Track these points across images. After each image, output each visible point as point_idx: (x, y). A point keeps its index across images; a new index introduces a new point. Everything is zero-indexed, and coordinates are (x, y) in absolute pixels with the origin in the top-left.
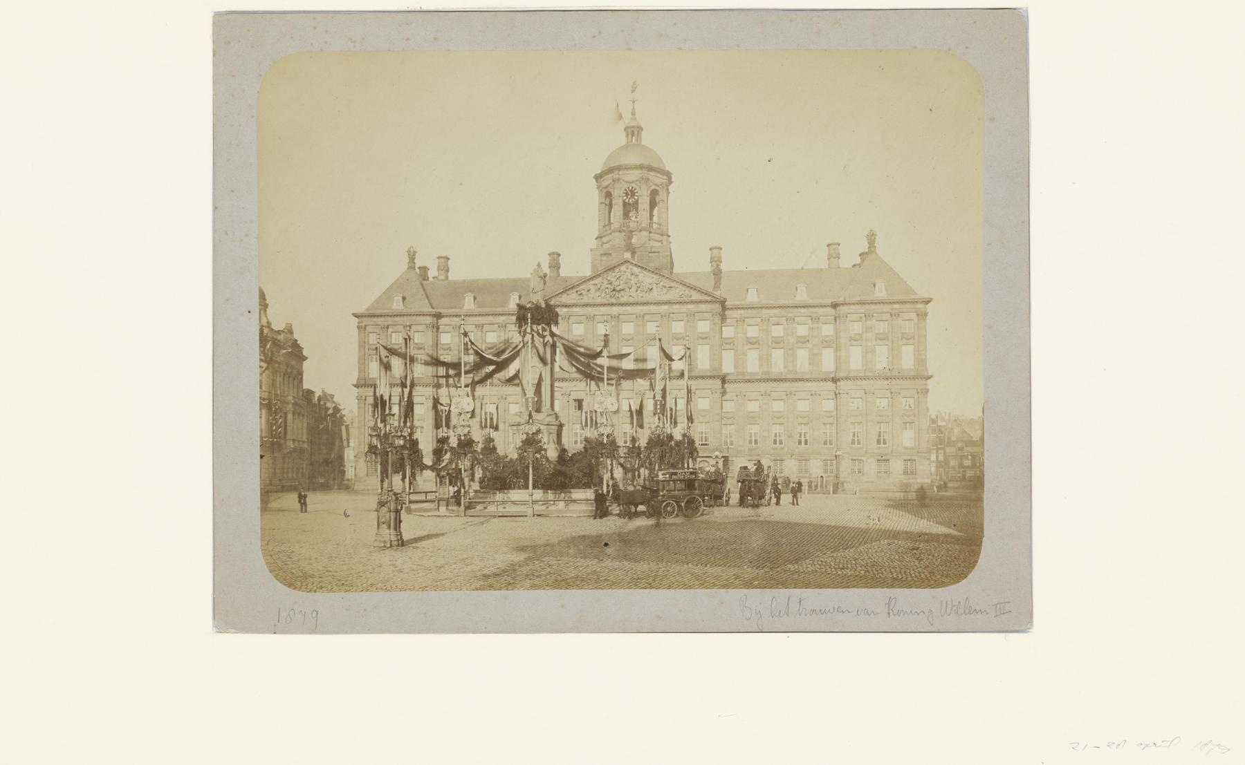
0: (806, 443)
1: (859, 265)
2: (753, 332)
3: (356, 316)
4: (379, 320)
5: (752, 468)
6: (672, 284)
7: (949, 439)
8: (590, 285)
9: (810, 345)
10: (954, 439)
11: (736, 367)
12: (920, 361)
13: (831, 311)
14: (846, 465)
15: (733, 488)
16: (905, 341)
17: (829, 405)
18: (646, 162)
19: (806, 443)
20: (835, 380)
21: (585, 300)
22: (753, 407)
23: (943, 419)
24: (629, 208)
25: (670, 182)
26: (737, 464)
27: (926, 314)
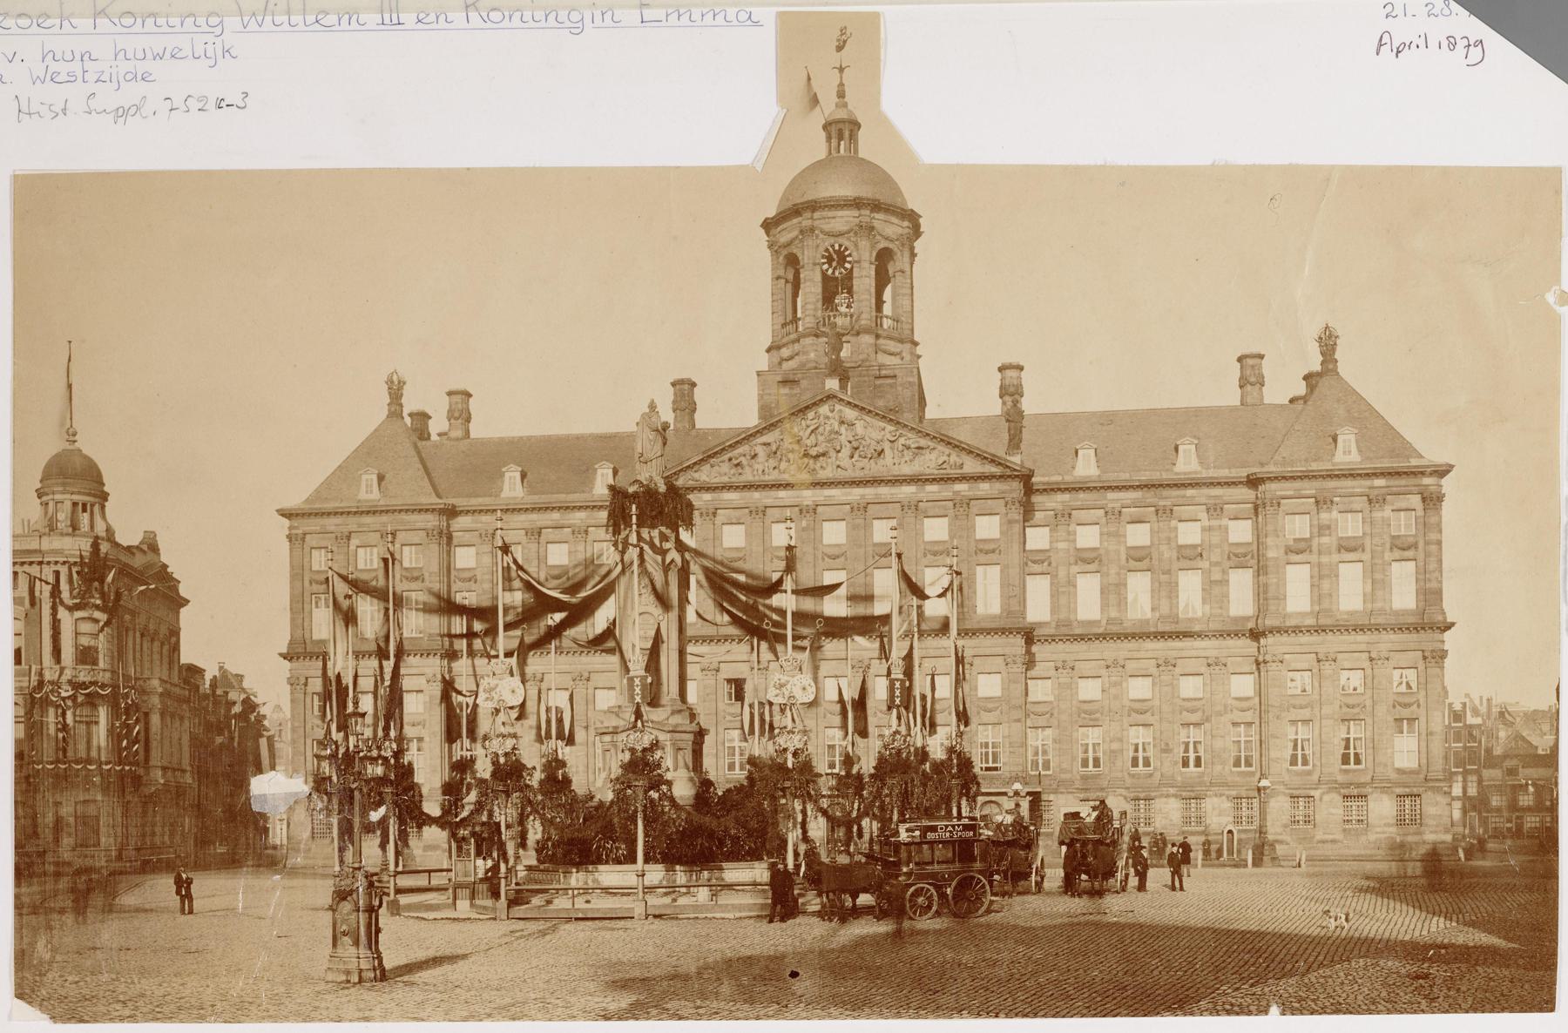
0: (1198, 763)
1: (1305, 399)
2: (1088, 537)
4: (331, 523)
5: (1088, 815)
6: (923, 442)
7: (1489, 751)
8: (757, 445)
9: (1205, 564)
10: (1498, 751)
11: (1055, 609)
12: (1430, 595)
14: (1279, 809)
15: (1050, 857)
16: (1397, 554)
17: (1243, 685)
18: (865, 192)
19: (1198, 763)
20: (1255, 635)
21: (748, 476)
22: (1089, 690)
23: (1476, 712)
24: (834, 288)
25: (916, 232)
26: (1059, 806)
27: (1440, 498)
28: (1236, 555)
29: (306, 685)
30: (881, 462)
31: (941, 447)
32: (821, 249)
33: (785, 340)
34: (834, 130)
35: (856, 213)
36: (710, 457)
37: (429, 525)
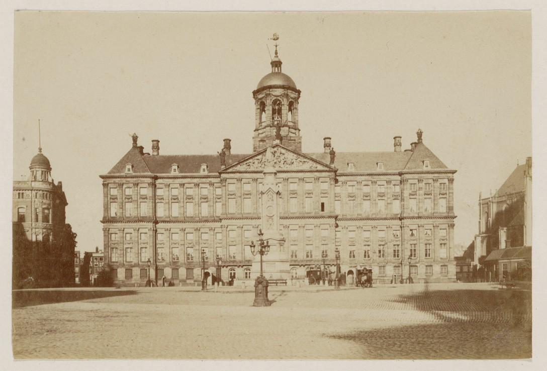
3: (102, 177)
4: (117, 180)
6: (305, 160)
8: (255, 160)
9: (386, 198)
12: (450, 209)
13: (399, 178)
16: (441, 196)
20: (401, 219)
21: (252, 169)
28: (395, 196)
29: (109, 230)
30: (292, 165)
31: (311, 162)
32: (272, 100)
33: (260, 128)
34: (274, 64)
35: (283, 90)
36: (240, 163)
37: (149, 182)
